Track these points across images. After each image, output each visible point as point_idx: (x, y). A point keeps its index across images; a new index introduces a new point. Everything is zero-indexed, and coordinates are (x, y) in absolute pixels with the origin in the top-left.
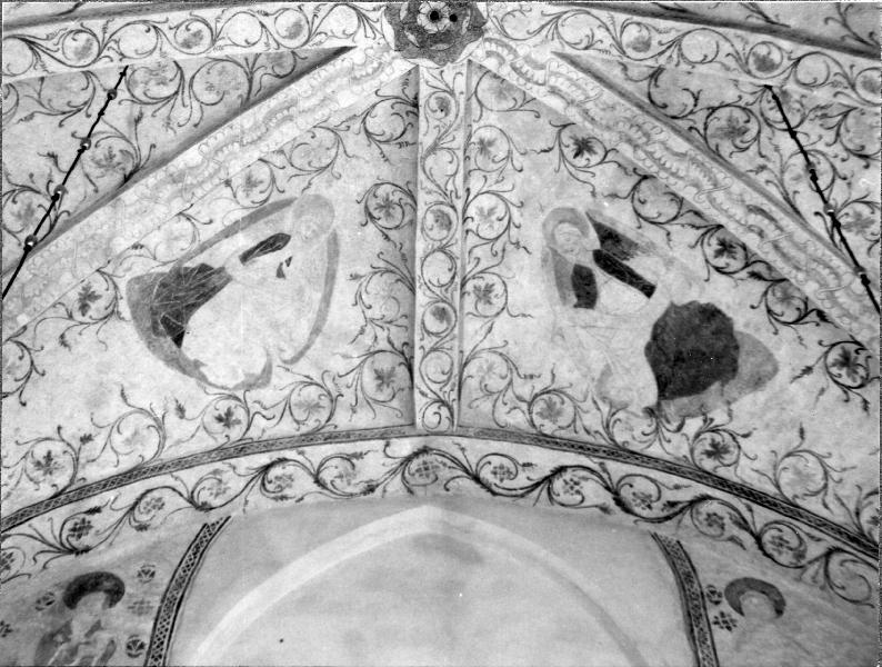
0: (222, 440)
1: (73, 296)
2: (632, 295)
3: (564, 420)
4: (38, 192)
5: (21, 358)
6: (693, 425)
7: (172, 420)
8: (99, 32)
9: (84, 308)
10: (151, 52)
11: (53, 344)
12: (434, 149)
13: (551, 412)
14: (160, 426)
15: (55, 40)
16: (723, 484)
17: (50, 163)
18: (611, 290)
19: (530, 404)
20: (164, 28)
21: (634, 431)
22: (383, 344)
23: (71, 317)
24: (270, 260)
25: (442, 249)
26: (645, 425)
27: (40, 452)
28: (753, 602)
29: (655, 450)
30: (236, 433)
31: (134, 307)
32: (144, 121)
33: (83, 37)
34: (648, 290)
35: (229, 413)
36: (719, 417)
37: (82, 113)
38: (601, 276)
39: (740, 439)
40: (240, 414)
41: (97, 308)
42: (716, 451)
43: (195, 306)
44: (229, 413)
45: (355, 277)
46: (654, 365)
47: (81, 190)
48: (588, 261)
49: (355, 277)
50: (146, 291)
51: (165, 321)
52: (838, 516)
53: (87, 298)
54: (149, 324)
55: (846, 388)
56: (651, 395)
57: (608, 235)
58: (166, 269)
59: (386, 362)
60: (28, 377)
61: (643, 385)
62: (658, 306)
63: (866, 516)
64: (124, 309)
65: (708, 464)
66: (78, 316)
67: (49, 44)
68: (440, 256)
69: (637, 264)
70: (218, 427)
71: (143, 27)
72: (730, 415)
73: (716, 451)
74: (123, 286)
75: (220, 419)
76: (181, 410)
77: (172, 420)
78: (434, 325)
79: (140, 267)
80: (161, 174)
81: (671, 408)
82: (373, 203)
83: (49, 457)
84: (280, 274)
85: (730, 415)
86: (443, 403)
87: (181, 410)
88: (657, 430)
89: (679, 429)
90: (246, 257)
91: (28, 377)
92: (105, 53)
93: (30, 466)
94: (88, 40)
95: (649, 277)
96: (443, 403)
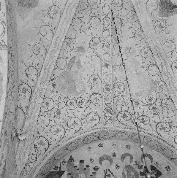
1: (158, 29)
4: (136, 32)
5: (168, 43)
8: (104, 17)
9: (162, 27)
10: (109, 6)
11: (168, 36)
15: (104, 26)
17: (130, 29)
20: (104, 3)
23: (163, 31)
31: (165, 16)
32: (126, 8)
33: (104, 21)
37: (123, 21)
41: (163, 24)
47: (137, 24)
50: (162, 13)
51: (171, 9)
53: (160, 26)
54: (170, 13)
58: (159, 7)
60: (173, 42)
66: (163, 29)
67: (105, 27)
71: (104, 8)
74: (161, 18)
79: (157, 13)
80: (135, 7)
91: (173, 42)
92: (108, 16)
94: (105, 19)
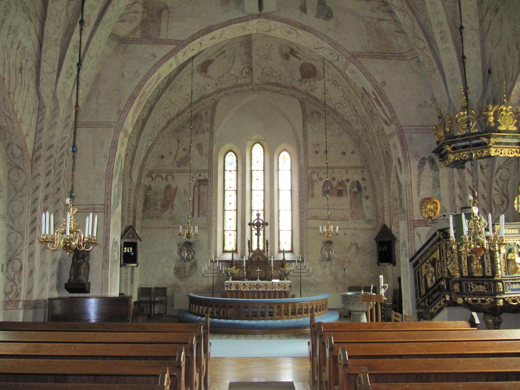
0: (217, 89)
2: (297, 60)
3: (283, 81)
6: (308, 84)
7: (207, 87)
12: (255, 40)
13: (280, 79)
14: (205, 88)
16: (312, 96)
18: (292, 58)
19: (276, 77)
21: (296, 84)
22: (246, 66)
24: (223, 55)
25: (258, 54)
26: (299, 83)
27: (185, 98)
28: (315, 116)
29: (300, 88)
30: (219, 87)
34: (300, 59)
35: (217, 84)
36: (312, 83)
38: (290, 55)
39: (316, 89)
40: (219, 83)
42: (312, 90)
43: (208, 67)
44: (217, 84)
45: (240, 55)
46: (301, 72)
48: (288, 53)
49: (240, 55)
52: (332, 106)
55: (336, 85)
56: (300, 77)
57: (292, 50)
59: (247, 70)
61: (298, 76)
62: (302, 62)
63: (336, 107)
64: (196, 71)
65: (310, 92)
68: (257, 56)
69: (297, 55)
70: (215, 86)
72: (315, 83)
73: (312, 90)
75: (216, 85)
76: (208, 85)
77: (207, 87)
78: (256, 66)
81: (304, 80)
82: (243, 43)
83: (186, 99)
84: (225, 57)
85: (315, 83)
86: (258, 79)
87: (208, 85)
88: (301, 84)
89: (305, 84)
90: (217, 57)
93: (183, 101)
95: (300, 57)
96: (258, 79)
